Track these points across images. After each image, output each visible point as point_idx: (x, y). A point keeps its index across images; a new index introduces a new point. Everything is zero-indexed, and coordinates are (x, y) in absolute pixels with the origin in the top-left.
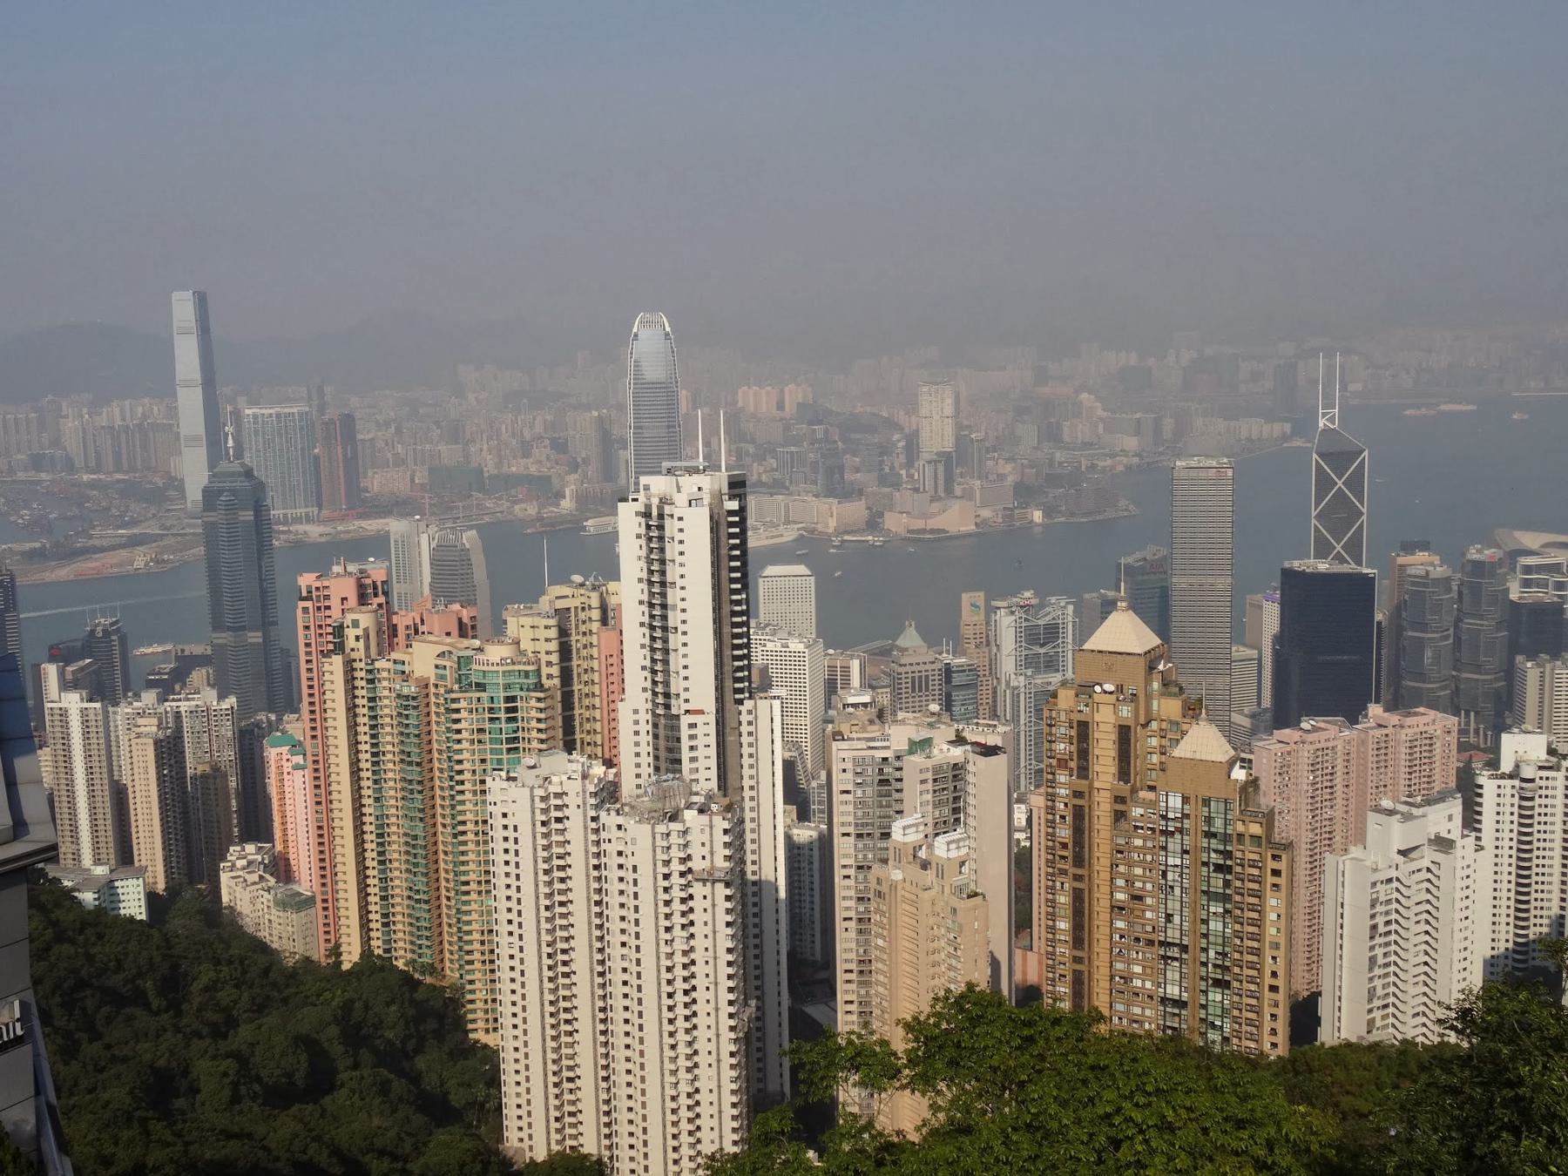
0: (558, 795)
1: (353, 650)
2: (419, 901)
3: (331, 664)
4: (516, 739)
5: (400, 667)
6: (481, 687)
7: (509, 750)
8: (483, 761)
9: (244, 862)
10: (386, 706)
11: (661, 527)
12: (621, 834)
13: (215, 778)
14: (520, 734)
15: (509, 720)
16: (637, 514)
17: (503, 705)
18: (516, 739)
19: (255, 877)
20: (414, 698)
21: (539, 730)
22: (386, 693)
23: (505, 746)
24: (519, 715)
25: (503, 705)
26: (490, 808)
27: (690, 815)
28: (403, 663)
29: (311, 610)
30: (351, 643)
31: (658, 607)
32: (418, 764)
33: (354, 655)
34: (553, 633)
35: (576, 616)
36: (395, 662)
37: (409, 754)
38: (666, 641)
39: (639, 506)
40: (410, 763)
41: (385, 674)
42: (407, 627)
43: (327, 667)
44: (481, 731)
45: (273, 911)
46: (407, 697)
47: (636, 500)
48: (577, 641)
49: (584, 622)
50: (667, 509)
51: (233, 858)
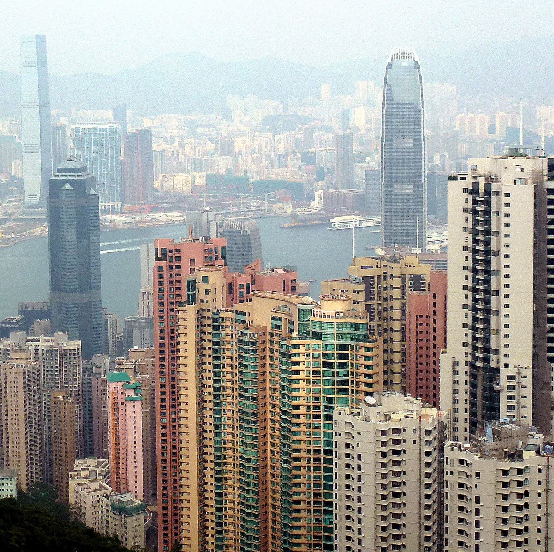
0: (397, 431)
1: (202, 301)
2: (249, 515)
3: (185, 312)
4: (346, 382)
5: (241, 317)
6: (317, 336)
7: (339, 391)
8: (316, 399)
9: (87, 473)
10: (228, 350)
11: (488, 203)
12: (462, 468)
13: (65, 404)
14: (349, 378)
15: (340, 365)
16: (465, 191)
17: (336, 352)
18: (346, 382)
19: (96, 485)
20: (254, 344)
21: (367, 376)
22: (228, 338)
23: (336, 387)
24: (349, 361)
25: (336, 352)
26: (335, 439)
27: (528, 455)
28: (244, 314)
29: (165, 268)
30: (202, 295)
31: (481, 273)
32: (254, 399)
33: (205, 306)
34: (361, 296)
35: (379, 283)
36: (237, 313)
37: (246, 390)
38: (487, 302)
39: (468, 184)
40: (247, 398)
41: (228, 323)
42: (241, 286)
43: (181, 315)
44: (316, 373)
45: (111, 514)
46: (247, 343)
47: (463, 179)
48: (379, 304)
49: (385, 289)
50: (494, 187)
51: (79, 469)
